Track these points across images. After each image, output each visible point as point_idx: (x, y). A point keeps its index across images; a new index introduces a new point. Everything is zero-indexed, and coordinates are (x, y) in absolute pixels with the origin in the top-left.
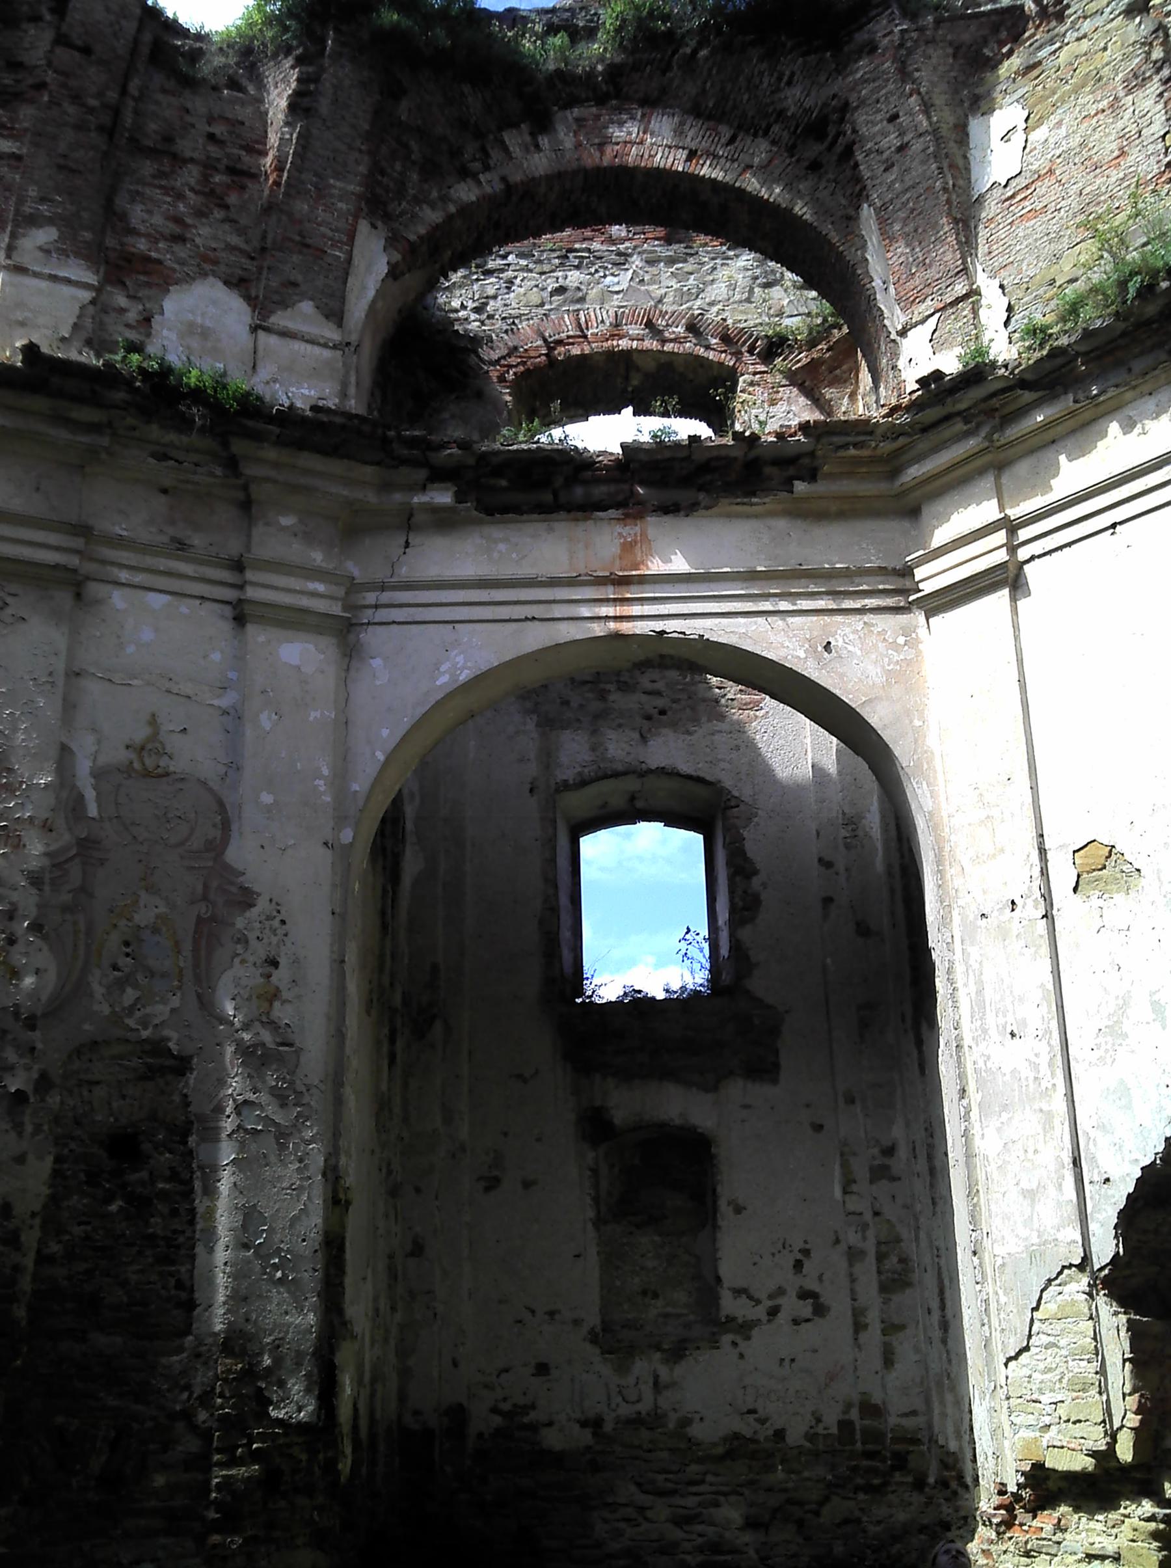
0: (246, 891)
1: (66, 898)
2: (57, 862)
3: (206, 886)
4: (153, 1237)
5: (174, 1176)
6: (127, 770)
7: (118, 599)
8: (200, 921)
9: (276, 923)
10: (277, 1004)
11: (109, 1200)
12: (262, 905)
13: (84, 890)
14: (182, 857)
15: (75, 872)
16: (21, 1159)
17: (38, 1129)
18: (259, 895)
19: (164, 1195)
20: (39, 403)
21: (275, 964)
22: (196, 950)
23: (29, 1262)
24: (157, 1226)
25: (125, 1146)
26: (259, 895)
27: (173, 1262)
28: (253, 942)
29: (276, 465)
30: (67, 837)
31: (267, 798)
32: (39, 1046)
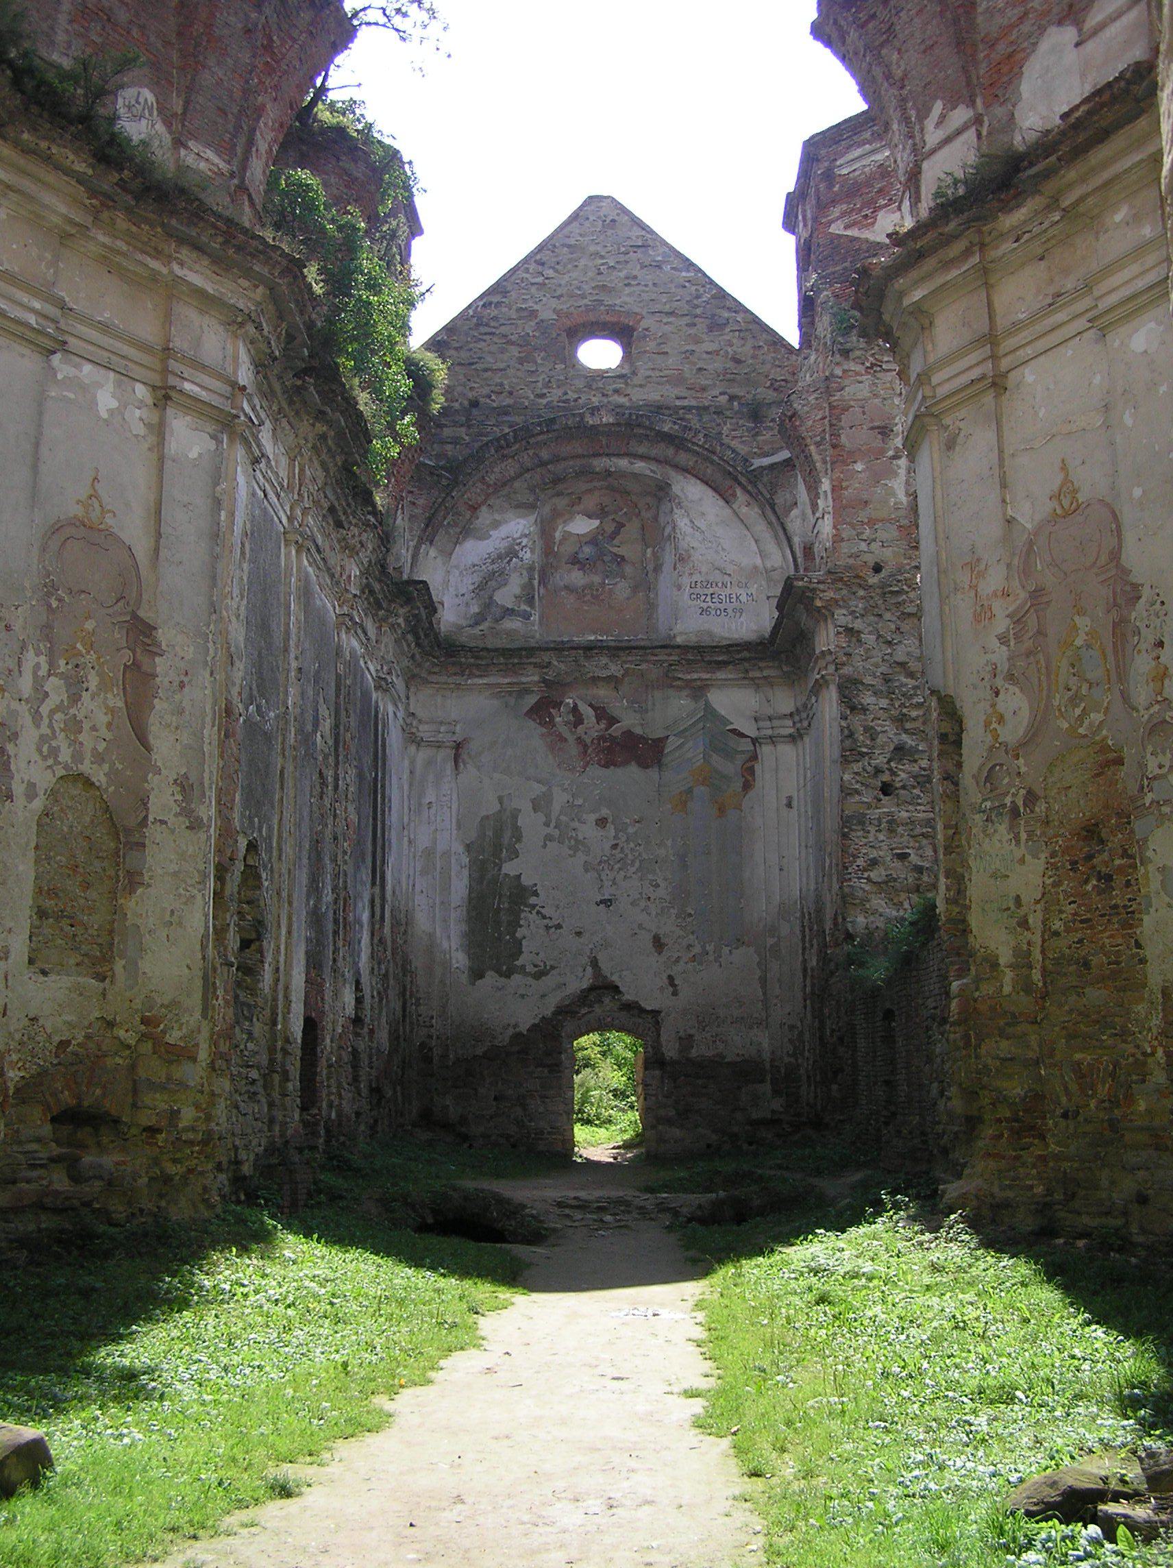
0: (1136, 587)
1: (1028, 644)
2: (1018, 620)
3: (1114, 593)
4: (1116, 907)
5: (1125, 854)
6: (1054, 518)
7: (1029, 375)
8: (1115, 625)
9: (1158, 605)
10: (1166, 682)
11: (1086, 881)
12: (1146, 593)
13: (1040, 633)
14: (1097, 575)
15: (1032, 622)
16: (1022, 861)
17: (1030, 834)
18: (1142, 585)
19: (1120, 869)
20: (930, 263)
21: (1161, 644)
22: (1116, 653)
23: (1037, 939)
24: (1118, 897)
25: (1091, 832)
26: (1142, 585)
27: (1131, 926)
28: (1144, 631)
29: (1083, 180)
30: (1023, 595)
31: (1137, 492)
32: (1023, 769)
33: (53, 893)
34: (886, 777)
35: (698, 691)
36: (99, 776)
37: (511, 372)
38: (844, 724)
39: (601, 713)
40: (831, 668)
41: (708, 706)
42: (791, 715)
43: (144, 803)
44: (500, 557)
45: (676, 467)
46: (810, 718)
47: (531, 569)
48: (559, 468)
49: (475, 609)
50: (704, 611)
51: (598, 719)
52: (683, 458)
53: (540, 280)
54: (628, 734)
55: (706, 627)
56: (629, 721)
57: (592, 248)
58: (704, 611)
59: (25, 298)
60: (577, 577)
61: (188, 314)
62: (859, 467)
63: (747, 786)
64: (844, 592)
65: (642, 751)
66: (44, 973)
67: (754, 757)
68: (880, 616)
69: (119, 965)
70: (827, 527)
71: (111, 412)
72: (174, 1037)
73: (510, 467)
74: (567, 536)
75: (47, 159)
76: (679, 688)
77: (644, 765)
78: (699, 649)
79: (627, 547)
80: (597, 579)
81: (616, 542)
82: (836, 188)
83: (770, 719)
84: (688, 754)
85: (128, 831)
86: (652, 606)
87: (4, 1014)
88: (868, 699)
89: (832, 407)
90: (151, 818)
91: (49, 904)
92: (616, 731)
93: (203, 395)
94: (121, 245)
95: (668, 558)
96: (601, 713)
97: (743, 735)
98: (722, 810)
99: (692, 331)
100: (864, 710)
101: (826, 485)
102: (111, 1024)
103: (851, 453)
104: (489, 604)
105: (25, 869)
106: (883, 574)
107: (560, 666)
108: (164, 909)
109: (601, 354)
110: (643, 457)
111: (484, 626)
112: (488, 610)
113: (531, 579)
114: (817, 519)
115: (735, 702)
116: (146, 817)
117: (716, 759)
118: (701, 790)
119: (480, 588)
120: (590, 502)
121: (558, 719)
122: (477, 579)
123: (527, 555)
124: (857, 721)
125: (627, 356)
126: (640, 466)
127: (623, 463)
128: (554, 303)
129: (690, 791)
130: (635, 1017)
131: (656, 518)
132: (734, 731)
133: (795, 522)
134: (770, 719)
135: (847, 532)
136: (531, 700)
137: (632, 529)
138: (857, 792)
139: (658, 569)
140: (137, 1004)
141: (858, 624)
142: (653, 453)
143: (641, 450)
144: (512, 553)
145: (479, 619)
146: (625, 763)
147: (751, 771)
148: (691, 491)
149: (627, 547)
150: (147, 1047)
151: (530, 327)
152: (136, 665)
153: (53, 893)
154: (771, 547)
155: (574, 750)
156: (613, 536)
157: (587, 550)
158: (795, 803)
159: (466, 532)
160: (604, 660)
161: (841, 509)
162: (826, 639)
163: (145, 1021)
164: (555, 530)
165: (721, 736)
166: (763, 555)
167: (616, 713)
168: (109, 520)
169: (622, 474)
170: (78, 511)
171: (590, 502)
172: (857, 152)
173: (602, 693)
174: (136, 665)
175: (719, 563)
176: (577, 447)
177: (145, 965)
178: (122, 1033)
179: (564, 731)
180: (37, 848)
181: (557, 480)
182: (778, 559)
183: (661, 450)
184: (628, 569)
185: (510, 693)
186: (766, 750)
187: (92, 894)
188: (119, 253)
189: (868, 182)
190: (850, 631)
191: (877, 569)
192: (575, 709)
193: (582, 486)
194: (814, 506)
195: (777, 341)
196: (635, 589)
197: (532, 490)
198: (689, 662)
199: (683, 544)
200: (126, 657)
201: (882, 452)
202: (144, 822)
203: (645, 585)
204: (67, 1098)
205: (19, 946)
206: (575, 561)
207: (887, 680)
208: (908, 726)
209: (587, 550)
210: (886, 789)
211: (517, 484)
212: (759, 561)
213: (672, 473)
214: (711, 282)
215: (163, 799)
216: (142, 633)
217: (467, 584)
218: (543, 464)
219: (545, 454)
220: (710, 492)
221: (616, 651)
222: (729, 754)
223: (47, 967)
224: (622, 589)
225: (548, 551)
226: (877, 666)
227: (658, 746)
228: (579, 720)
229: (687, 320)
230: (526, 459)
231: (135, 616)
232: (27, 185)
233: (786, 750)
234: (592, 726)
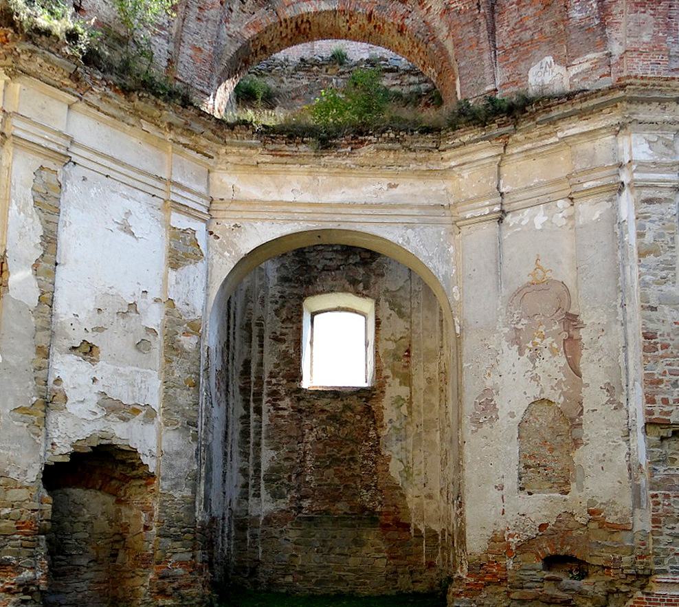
33: (532, 456)
59: (480, 204)
61: (586, 146)
66: (530, 494)
69: (573, 486)
71: (544, 224)
72: (611, 519)
85: (572, 420)
87: (503, 514)
90: (585, 410)
91: (530, 462)
93: (599, 183)
94: (529, 146)
102: (572, 515)
105: (514, 449)
108: (598, 455)
116: (582, 410)
140: (585, 504)
150: (593, 525)
152: (570, 338)
153: (532, 456)
163: (591, 513)
168: (548, 275)
170: (530, 279)
174: (570, 338)
177: (588, 483)
178: (578, 519)
180: (519, 437)
187: (556, 453)
188: (530, 150)
200: (565, 335)
202: (581, 413)
204: (549, 551)
205: (511, 483)
215: (593, 397)
216: (572, 320)
223: (531, 491)
231: (567, 314)
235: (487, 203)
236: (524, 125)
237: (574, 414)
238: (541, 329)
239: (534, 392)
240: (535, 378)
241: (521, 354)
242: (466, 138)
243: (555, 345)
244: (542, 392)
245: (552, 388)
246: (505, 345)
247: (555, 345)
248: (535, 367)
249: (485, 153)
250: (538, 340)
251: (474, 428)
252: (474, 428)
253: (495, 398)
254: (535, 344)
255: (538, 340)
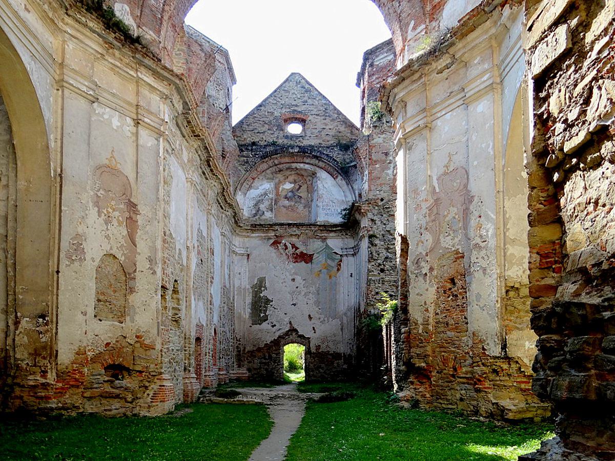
34: (382, 267)
35: (324, 239)
36: (118, 256)
37: (266, 133)
38: (369, 249)
39: (293, 246)
40: (366, 232)
41: (327, 245)
42: (353, 248)
43: (135, 265)
44: (262, 195)
45: (318, 167)
46: (359, 249)
47: (272, 199)
48: (281, 166)
49: (254, 212)
50: (327, 214)
51: (293, 248)
52: (321, 164)
53: (275, 102)
54: (302, 252)
55: (327, 219)
56: (302, 249)
57: (293, 91)
58: (327, 214)
60: (286, 203)
62: (377, 166)
63: (338, 270)
64: (371, 207)
65: (306, 258)
67: (341, 261)
68: (382, 215)
70: (366, 186)
73: (265, 166)
74: (283, 189)
75: (86, 26)
76: (318, 239)
77: (307, 263)
78: (324, 226)
79: (303, 193)
80: (293, 203)
81: (299, 191)
82: (374, 69)
83: (346, 249)
84: (320, 260)
86: (310, 212)
88: (377, 242)
89: (369, 146)
90: (137, 270)
92: (298, 252)
95: (315, 198)
96: (293, 246)
97: (337, 254)
98: (330, 277)
99: (325, 121)
100: (376, 245)
101: (367, 172)
103: (375, 161)
104: (258, 210)
106: (384, 201)
107: (280, 231)
109: (295, 129)
110: (308, 163)
111: (257, 217)
112: (258, 212)
113: (272, 202)
114: (364, 184)
115: (336, 243)
117: (329, 262)
118: (324, 271)
119: (256, 205)
120: (291, 178)
121: (280, 247)
122: (255, 202)
123: (271, 196)
124: (373, 249)
125: (304, 130)
126: (307, 166)
127: (302, 165)
128: (279, 110)
129: (320, 271)
130: (302, 339)
131: (312, 184)
132: (334, 252)
133: (355, 187)
134: (346, 249)
135: (373, 188)
136: (272, 241)
137: (304, 187)
138: (373, 271)
139: (312, 201)
141: (375, 218)
142: (311, 162)
143: (307, 161)
144: (266, 194)
145: (255, 215)
146: (301, 261)
147: (340, 265)
148: (322, 174)
149: (303, 193)
151: (272, 118)
154: (348, 194)
155: (285, 257)
156: (298, 190)
157: (290, 194)
158: (353, 275)
159: (250, 187)
160: (294, 229)
161: (370, 180)
162: (365, 223)
164: (279, 187)
165: (331, 254)
166: (345, 196)
167: (298, 246)
169: (301, 169)
171: (291, 178)
172: (382, 56)
173: (294, 240)
175: (330, 197)
176: (287, 160)
179: (282, 251)
181: (280, 171)
182: (350, 199)
183: (314, 161)
184: (303, 201)
185: (265, 239)
186: (344, 258)
189: (385, 67)
190: (372, 220)
191: (382, 200)
192: (285, 245)
193: (288, 173)
194: (363, 179)
195: (352, 126)
196: (305, 207)
197: (272, 173)
198: (321, 230)
199: (320, 192)
201: (386, 161)
202: (135, 271)
203: (308, 206)
206: (286, 197)
207: (383, 236)
208: (389, 251)
209: (290, 194)
210: (382, 271)
211: (268, 171)
212: (344, 199)
213: (317, 169)
214: (332, 104)
215: (142, 264)
217: (252, 203)
218: (276, 165)
219: (276, 162)
220: (330, 176)
221: (298, 225)
222: (333, 260)
224: (301, 207)
225: (277, 194)
226: (380, 231)
227: (311, 256)
228: (286, 248)
229: (323, 117)
230: (270, 163)
232: (78, 35)
233: (351, 259)
234: (290, 250)
235: (86, 84)
236: (126, 50)
237: (131, 271)
238: (113, 203)
239: (106, 248)
240: (107, 237)
241: (99, 216)
242: (91, 24)
243: (120, 218)
244: (111, 249)
245: (118, 248)
246: (91, 204)
247: (120, 218)
248: (107, 229)
249: (94, 44)
250: (110, 210)
251: (67, 263)
252: (67, 263)
253: (84, 243)
254: (108, 212)
255: (110, 210)
